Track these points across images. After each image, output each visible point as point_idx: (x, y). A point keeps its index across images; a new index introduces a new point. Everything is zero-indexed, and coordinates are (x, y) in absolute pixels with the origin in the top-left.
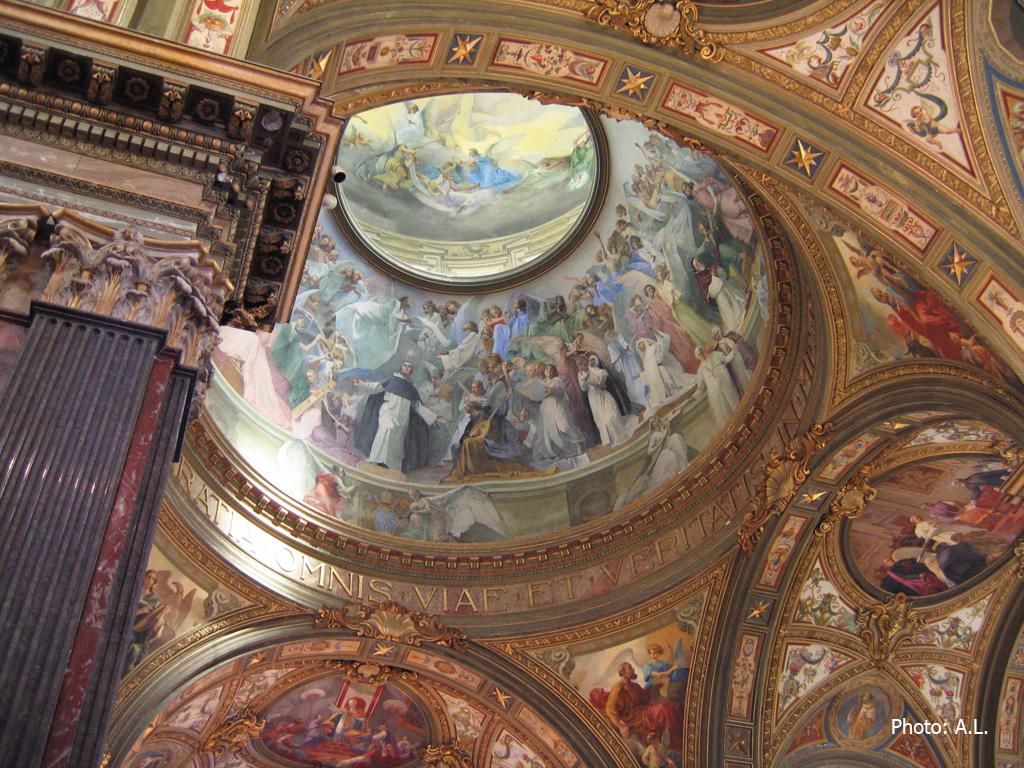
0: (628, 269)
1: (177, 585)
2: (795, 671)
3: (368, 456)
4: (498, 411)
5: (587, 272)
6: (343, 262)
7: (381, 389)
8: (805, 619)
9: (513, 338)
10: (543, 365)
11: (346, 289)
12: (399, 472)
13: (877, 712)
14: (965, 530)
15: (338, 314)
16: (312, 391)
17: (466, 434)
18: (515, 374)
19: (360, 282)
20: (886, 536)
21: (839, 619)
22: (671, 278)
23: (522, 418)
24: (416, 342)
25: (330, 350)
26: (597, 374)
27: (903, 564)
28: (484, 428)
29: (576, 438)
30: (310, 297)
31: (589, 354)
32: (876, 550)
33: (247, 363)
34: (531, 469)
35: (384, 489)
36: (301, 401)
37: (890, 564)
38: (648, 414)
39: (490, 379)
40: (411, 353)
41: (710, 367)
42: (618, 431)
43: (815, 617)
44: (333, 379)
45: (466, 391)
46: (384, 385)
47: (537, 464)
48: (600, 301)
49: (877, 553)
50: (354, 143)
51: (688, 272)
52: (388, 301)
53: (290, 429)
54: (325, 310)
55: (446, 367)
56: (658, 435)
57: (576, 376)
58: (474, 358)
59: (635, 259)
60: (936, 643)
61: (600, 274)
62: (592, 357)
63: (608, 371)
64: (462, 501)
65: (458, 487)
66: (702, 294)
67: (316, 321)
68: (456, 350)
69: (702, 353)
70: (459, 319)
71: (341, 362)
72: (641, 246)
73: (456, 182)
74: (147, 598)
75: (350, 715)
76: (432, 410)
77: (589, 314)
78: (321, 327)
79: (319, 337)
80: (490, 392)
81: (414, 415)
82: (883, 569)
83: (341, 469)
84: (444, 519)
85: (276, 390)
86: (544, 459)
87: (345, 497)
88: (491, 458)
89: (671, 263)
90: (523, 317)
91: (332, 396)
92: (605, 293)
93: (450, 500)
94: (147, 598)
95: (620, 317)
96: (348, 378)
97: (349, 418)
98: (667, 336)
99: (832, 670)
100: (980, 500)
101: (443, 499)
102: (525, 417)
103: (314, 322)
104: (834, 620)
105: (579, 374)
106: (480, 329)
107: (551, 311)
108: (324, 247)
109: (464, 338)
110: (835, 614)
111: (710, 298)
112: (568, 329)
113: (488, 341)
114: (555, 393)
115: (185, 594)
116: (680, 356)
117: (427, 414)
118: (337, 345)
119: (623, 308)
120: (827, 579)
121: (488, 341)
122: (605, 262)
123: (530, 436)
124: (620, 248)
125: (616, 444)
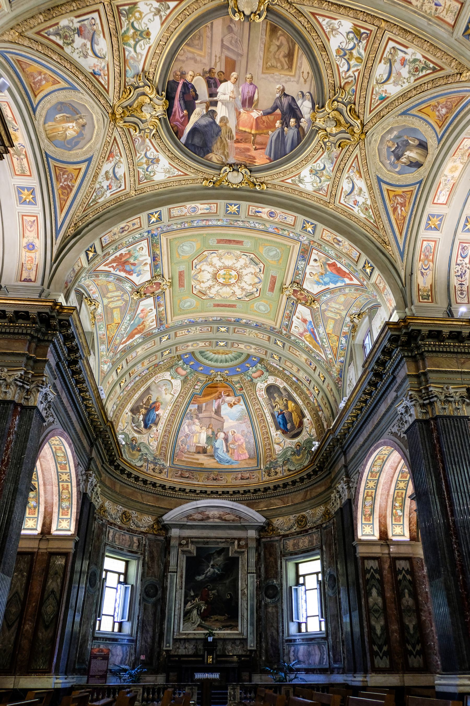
2: (80, 32)
8: (123, 19)
13: (74, 138)
14: (232, 124)
20: (213, 58)
21: (132, 58)
27: (191, 90)
32: (198, 58)
37: (189, 78)
43: (128, 29)
49: (196, 61)
60: (138, 155)
82: (183, 75)
99: (94, 74)
100: (264, 118)
104: (130, 52)
110: (135, 51)
120: (162, 24)
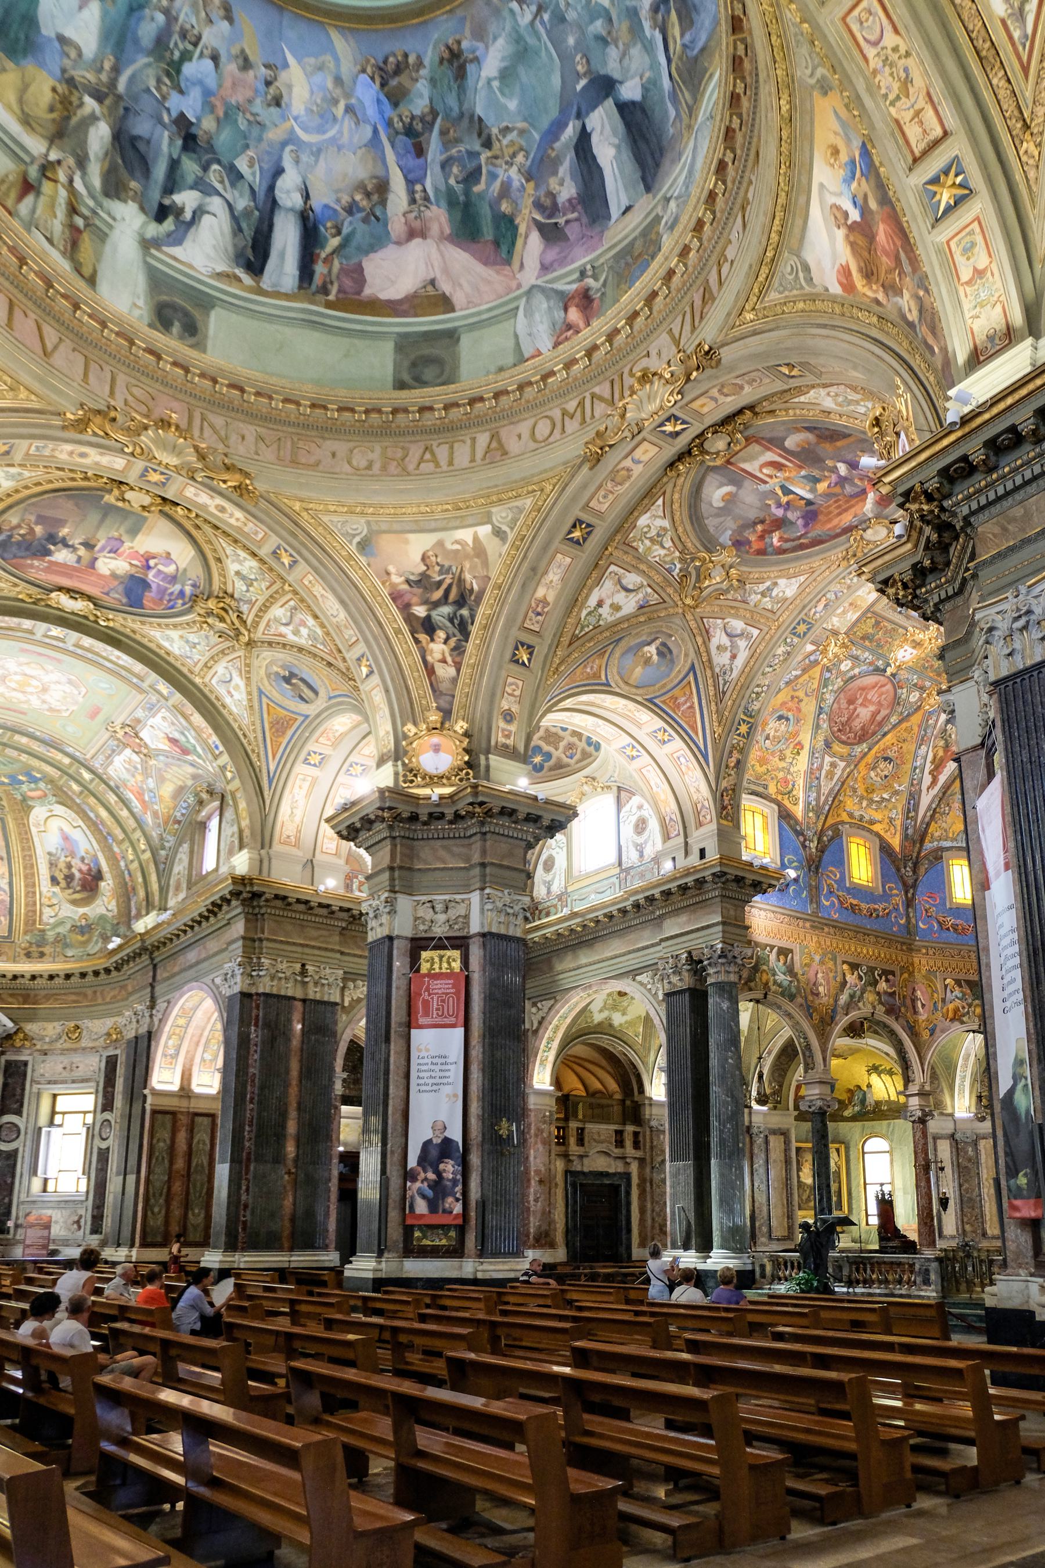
1: (457, 542)
15: (479, 111)
25: (503, 157)
30: (443, 133)
44: (528, 181)
54: (465, 122)
71: (522, 153)
74: (440, 573)
75: (787, 479)
78: (477, 147)
91: (539, 199)
94: (440, 573)
115: (470, 543)
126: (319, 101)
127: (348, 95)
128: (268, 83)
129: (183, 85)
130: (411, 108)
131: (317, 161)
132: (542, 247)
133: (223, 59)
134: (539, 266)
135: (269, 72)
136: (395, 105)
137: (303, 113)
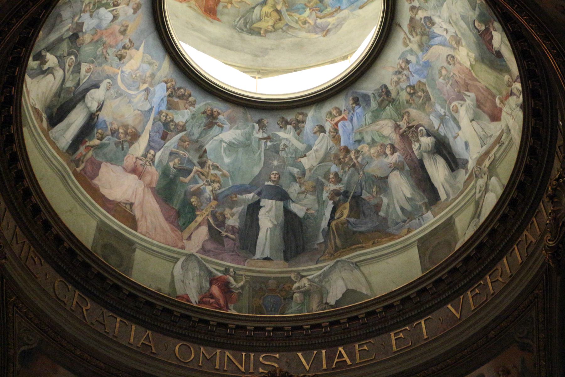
0: (430, 47)
3: (254, 254)
4: (355, 192)
5: (400, 58)
6: (202, 104)
7: (257, 198)
9: (355, 129)
10: (383, 146)
11: (210, 126)
12: (282, 262)
15: (208, 147)
16: (197, 213)
17: (332, 218)
18: (362, 160)
19: (221, 117)
22: (464, 44)
23: (374, 194)
24: (277, 152)
26: (427, 141)
28: (345, 211)
29: (421, 200)
30: (182, 140)
31: (417, 127)
33: (136, 204)
34: (391, 236)
35: (270, 278)
36: (190, 222)
38: (471, 165)
39: (343, 169)
40: (275, 163)
41: (510, 112)
42: (452, 186)
44: (214, 199)
45: (326, 183)
46: (259, 194)
47: (392, 230)
48: (415, 80)
50: (231, 3)
51: (473, 33)
52: (248, 126)
53: (183, 248)
54: (197, 146)
55: (307, 167)
56: (481, 182)
57: (411, 148)
58: (327, 154)
59: (432, 36)
61: (410, 57)
62: (421, 128)
63: (435, 137)
64: (334, 276)
65: (331, 263)
66: (489, 49)
67: (191, 157)
68: (312, 151)
69: (502, 102)
70: (309, 126)
71: (218, 184)
72: (433, 24)
73: (321, 11)
76: (301, 205)
77: (409, 94)
78: (195, 161)
79: (195, 168)
80: (345, 179)
81: (287, 212)
83: (232, 270)
84: (322, 293)
85: (167, 219)
86: (397, 224)
87: (237, 292)
88: (354, 233)
89: (459, 30)
90: (359, 110)
91: (216, 212)
92: (417, 72)
93: (325, 275)
95: (433, 88)
96: (227, 196)
97: (233, 227)
98: (472, 95)
101: (320, 275)
102: (377, 192)
103: (188, 158)
105: (413, 146)
106: (327, 130)
107: (380, 99)
108: (181, 97)
109: (316, 140)
111: (496, 51)
112: (396, 109)
113: (336, 138)
114: (397, 167)
116: (486, 109)
117: (298, 209)
118: (212, 172)
119: (433, 79)
121: (336, 138)
122: (411, 45)
123: (384, 207)
124: (419, 30)
125: (452, 197)
126: (138, 75)
127: (152, 85)
128: (124, 47)
129: (94, 14)
130: (175, 116)
131: (116, 98)
132: (207, 238)
133: (117, 21)
134: (200, 247)
135: (129, 44)
136: (169, 109)
137: (127, 73)
